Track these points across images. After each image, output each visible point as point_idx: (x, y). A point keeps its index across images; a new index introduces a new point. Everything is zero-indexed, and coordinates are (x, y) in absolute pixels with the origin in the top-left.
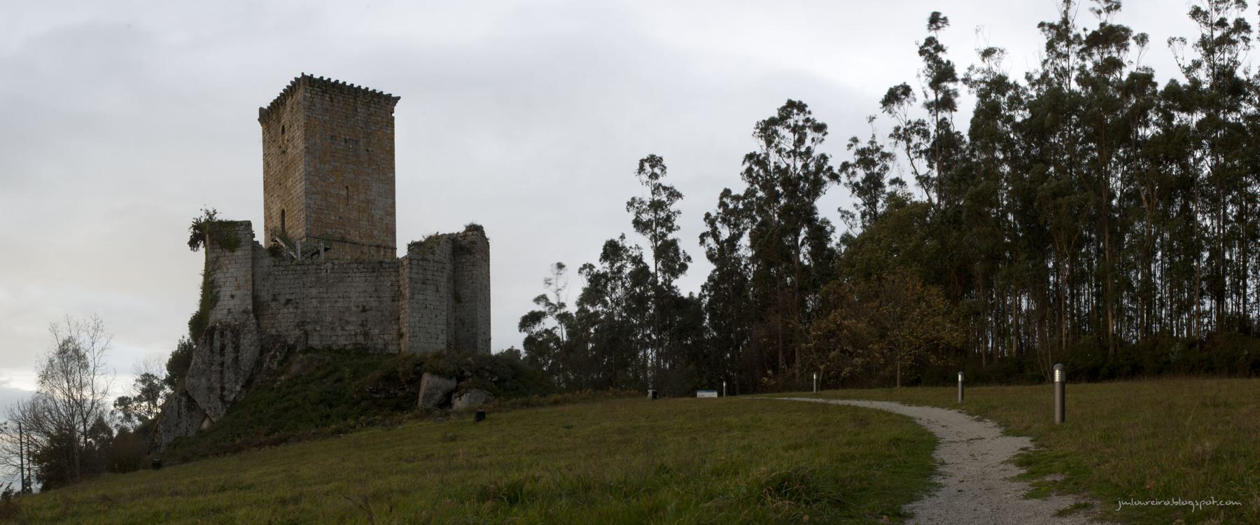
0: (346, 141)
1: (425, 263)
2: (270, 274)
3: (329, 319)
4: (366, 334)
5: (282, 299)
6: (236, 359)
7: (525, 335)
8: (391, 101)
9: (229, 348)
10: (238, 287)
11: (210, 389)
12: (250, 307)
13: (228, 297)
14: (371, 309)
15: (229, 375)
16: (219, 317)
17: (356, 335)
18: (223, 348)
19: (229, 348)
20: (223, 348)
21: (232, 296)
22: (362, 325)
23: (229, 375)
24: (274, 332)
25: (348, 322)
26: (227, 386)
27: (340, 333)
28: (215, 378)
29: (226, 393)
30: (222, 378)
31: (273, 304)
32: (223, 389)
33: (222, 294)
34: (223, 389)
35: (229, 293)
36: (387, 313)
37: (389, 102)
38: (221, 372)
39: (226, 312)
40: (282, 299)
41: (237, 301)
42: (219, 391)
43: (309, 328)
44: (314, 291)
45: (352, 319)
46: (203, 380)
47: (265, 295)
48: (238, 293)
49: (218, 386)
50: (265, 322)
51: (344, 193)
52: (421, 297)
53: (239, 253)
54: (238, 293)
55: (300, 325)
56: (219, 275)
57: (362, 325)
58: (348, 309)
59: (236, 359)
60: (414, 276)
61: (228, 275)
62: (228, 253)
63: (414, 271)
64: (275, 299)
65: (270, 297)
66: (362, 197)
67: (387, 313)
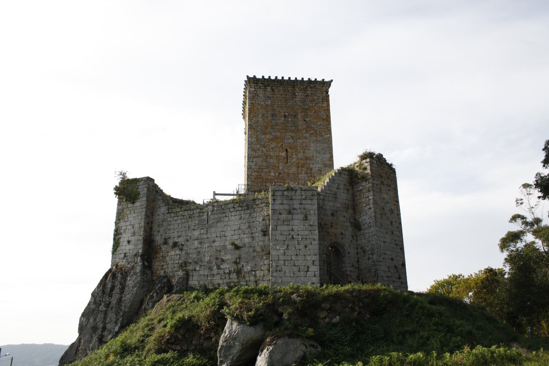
0: (285, 116)
1: (290, 194)
2: (164, 221)
3: (207, 259)
4: (239, 272)
5: (171, 242)
6: (120, 301)
7: (505, 254)
8: (325, 85)
9: (117, 290)
10: (134, 234)
11: (94, 329)
12: (140, 251)
13: (125, 243)
14: (245, 245)
15: (111, 315)
16: (117, 260)
17: (229, 273)
18: (112, 289)
19: (117, 290)
20: (112, 289)
21: (129, 242)
22: (236, 263)
23: (111, 315)
24: (162, 273)
25: (223, 261)
26: (109, 326)
27: (215, 271)
28: (100, 316)
29: (106, 333)
30: (105, 318)
31: (164, 248)
32: (104, 328)
33: (122, 240)
34: (104, 328)
35: (126, 239)
36: (258, 249)
37: (325, 85)
38: (106, 314)
39: (122, 255)
40: (171, 242)
41: (131, 246)
42: (99, 332)
43: (190, 267)
44: (196, 233)
45: (227, 257)
46: (91, 320)
47: (159, 239)
48: (133, 239)
49: (101, 325)
50: (156, 265)
51: (284, 154)
52: (285, 228)
53: (137, 204)
54: (133, 239)
55: (184, 265)
56: (122, 224)
57: (236, 263)
58: (224, 247)
59: (120, 301)
60: (277, 207)
61: (128, 223)
62: (130, 205)
63: (278, 202)
64: (166, 243)
65: (163, 241)
66: (300, 155)
67: (258, 249)
